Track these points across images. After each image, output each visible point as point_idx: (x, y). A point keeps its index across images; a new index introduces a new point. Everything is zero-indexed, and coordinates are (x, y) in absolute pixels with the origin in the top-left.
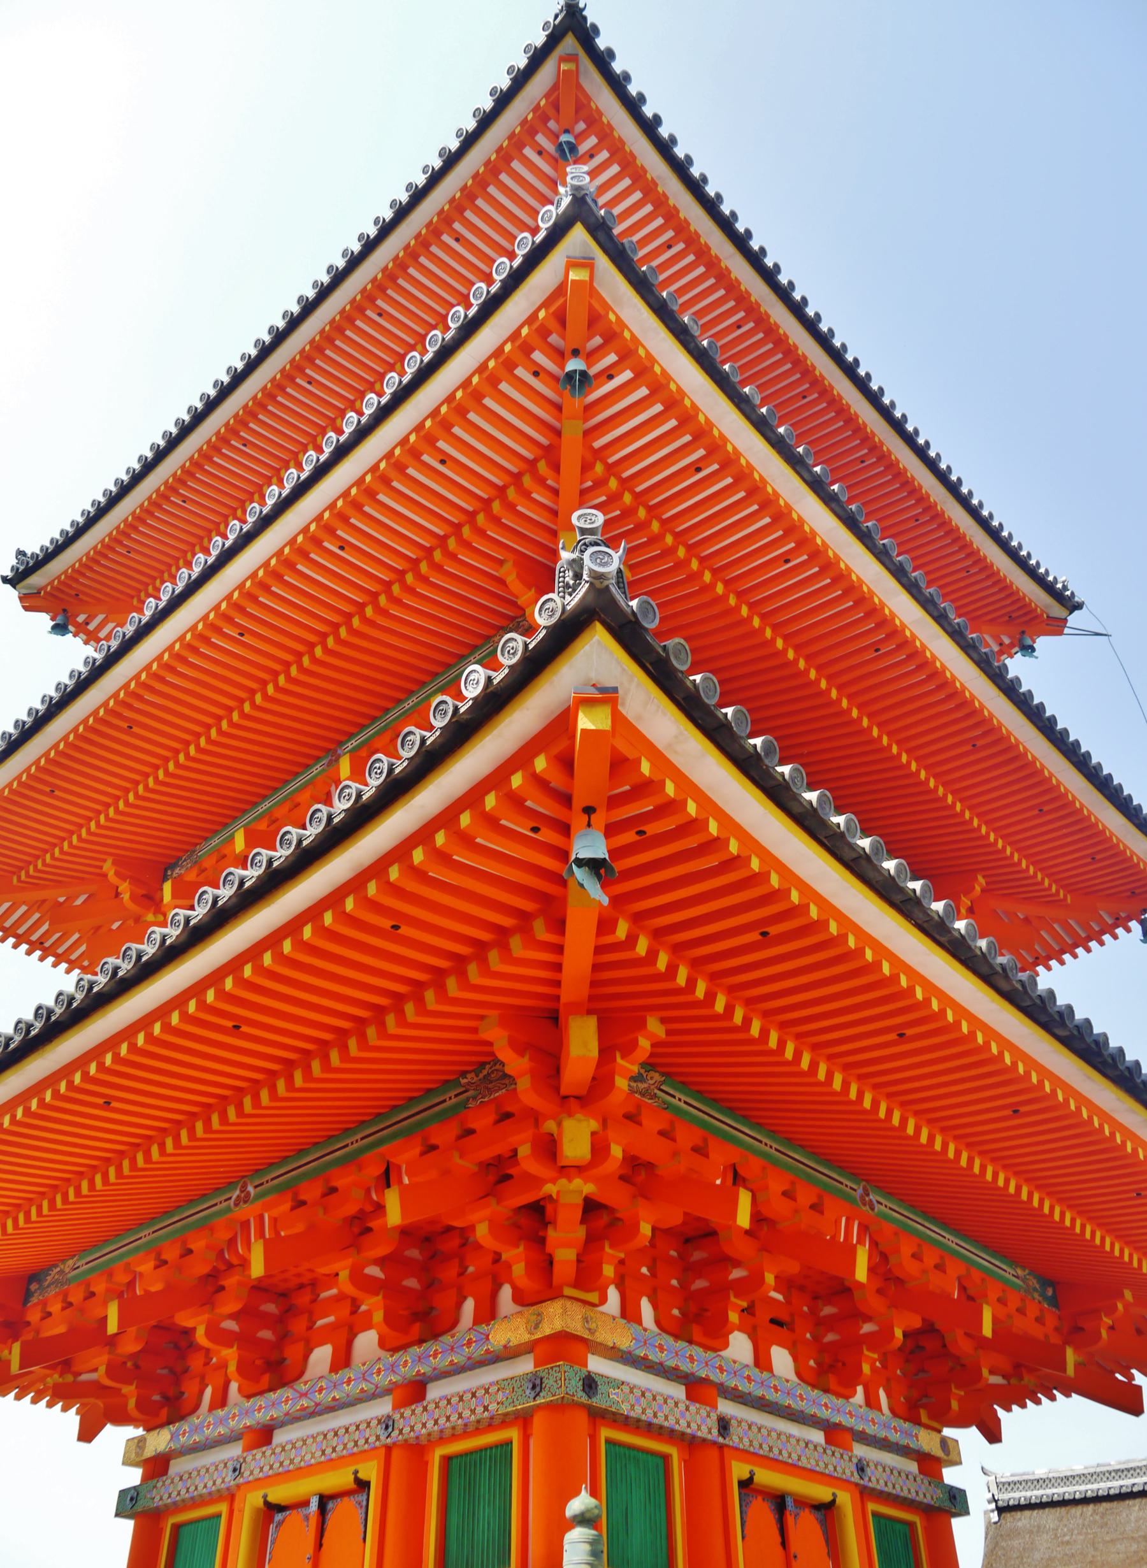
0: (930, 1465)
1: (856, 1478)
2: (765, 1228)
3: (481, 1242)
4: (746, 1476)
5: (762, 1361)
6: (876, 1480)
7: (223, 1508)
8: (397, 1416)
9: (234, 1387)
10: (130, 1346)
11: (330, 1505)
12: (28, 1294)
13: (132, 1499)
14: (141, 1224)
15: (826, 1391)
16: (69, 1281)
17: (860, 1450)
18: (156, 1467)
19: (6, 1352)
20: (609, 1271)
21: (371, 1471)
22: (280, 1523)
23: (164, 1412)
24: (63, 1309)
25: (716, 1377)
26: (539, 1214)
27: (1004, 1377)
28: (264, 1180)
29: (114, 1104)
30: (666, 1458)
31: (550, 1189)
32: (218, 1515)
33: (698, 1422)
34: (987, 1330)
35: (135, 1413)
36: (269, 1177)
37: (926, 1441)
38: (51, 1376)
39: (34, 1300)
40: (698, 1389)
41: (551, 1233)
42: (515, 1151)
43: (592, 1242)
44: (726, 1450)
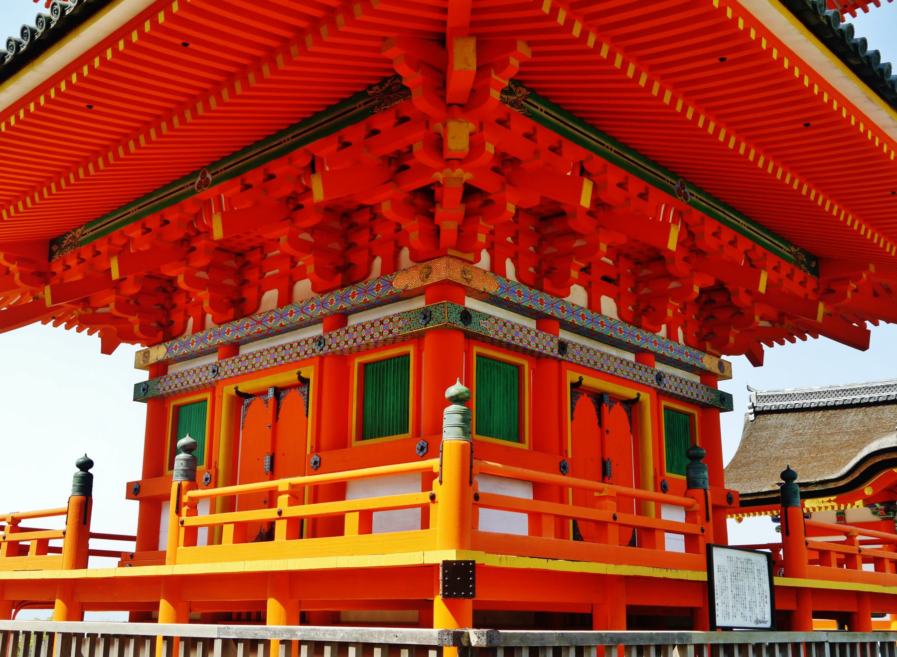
0: (709, 378)
1: (655, 384)
5: (594, 305)
6: (670, 386)
7: (208, 395)
8: (327, 337)
9: (209, 317)
10: (130, 289)
11: (282, 394)
12: (51, 254)
13: (144, 390)
14: (129, 204)
15: (639, 327)
16: (80, 244)
17: (659, 367)
18: (159, 370)
19: (41, 293)
20: (482, 238)
21: (309, 372)
22: (248, 405)
23: (161, 334)
24: (78, 263)
25: (558, 314)
26: (428, 196)
27: (770, 322)
28: (219, 169)
30: (520, 367)
31: (439, 176)
32: (205, 400)
33: (545, 344)
34: (762, 288)
35: (140, 335)
37: (709, 363)
38: (76, 309)
39: (56, 257)
40: (544, 321)
41: (439, 211)
42: (411, 147)
43: (469, 215)
44: (563, 363)
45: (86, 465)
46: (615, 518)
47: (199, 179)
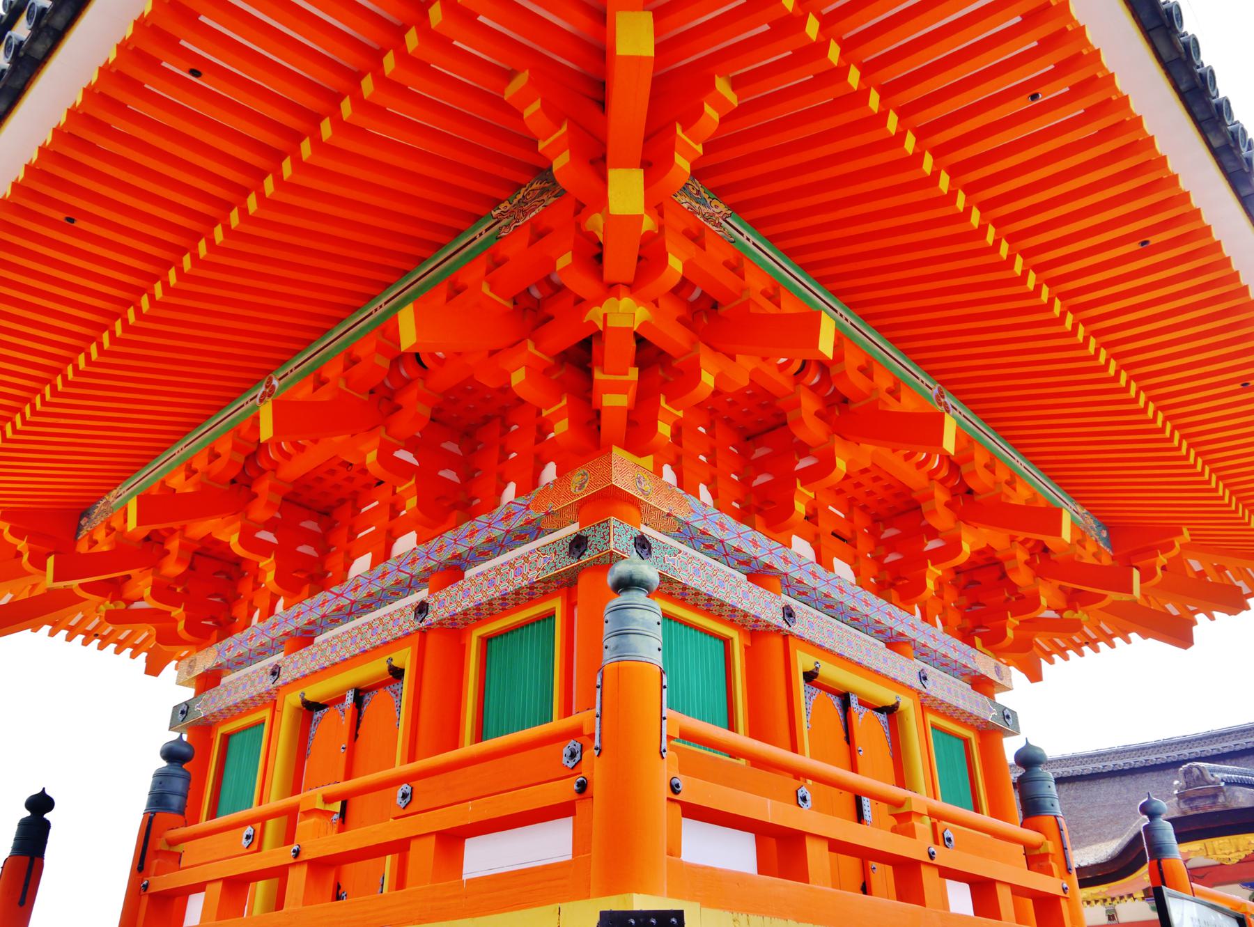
1: (917, 684)
2: (837, 413)
3: (520, 393)
4: (811, 667)
8: (430, 601)
11: (367, 697)
12: (79, 528)
15: (890, 602)
21: (404, 658)
24: (107, 535)
25: (779, 565)
26: (581, 357)
27: (1056, 611)
28: (288, 370)
29: (80, 224)
30: (727, 642)
33: (764, 605)
35: (185, 636)
36: (292, 367)
38: (102, 603)
39: (84, 533)
44: (790, 638)
45: (41, 803)
46: (931, 855)
47: (263, 389)
